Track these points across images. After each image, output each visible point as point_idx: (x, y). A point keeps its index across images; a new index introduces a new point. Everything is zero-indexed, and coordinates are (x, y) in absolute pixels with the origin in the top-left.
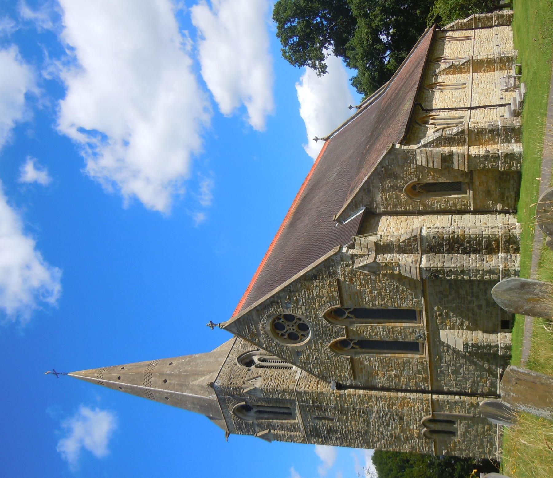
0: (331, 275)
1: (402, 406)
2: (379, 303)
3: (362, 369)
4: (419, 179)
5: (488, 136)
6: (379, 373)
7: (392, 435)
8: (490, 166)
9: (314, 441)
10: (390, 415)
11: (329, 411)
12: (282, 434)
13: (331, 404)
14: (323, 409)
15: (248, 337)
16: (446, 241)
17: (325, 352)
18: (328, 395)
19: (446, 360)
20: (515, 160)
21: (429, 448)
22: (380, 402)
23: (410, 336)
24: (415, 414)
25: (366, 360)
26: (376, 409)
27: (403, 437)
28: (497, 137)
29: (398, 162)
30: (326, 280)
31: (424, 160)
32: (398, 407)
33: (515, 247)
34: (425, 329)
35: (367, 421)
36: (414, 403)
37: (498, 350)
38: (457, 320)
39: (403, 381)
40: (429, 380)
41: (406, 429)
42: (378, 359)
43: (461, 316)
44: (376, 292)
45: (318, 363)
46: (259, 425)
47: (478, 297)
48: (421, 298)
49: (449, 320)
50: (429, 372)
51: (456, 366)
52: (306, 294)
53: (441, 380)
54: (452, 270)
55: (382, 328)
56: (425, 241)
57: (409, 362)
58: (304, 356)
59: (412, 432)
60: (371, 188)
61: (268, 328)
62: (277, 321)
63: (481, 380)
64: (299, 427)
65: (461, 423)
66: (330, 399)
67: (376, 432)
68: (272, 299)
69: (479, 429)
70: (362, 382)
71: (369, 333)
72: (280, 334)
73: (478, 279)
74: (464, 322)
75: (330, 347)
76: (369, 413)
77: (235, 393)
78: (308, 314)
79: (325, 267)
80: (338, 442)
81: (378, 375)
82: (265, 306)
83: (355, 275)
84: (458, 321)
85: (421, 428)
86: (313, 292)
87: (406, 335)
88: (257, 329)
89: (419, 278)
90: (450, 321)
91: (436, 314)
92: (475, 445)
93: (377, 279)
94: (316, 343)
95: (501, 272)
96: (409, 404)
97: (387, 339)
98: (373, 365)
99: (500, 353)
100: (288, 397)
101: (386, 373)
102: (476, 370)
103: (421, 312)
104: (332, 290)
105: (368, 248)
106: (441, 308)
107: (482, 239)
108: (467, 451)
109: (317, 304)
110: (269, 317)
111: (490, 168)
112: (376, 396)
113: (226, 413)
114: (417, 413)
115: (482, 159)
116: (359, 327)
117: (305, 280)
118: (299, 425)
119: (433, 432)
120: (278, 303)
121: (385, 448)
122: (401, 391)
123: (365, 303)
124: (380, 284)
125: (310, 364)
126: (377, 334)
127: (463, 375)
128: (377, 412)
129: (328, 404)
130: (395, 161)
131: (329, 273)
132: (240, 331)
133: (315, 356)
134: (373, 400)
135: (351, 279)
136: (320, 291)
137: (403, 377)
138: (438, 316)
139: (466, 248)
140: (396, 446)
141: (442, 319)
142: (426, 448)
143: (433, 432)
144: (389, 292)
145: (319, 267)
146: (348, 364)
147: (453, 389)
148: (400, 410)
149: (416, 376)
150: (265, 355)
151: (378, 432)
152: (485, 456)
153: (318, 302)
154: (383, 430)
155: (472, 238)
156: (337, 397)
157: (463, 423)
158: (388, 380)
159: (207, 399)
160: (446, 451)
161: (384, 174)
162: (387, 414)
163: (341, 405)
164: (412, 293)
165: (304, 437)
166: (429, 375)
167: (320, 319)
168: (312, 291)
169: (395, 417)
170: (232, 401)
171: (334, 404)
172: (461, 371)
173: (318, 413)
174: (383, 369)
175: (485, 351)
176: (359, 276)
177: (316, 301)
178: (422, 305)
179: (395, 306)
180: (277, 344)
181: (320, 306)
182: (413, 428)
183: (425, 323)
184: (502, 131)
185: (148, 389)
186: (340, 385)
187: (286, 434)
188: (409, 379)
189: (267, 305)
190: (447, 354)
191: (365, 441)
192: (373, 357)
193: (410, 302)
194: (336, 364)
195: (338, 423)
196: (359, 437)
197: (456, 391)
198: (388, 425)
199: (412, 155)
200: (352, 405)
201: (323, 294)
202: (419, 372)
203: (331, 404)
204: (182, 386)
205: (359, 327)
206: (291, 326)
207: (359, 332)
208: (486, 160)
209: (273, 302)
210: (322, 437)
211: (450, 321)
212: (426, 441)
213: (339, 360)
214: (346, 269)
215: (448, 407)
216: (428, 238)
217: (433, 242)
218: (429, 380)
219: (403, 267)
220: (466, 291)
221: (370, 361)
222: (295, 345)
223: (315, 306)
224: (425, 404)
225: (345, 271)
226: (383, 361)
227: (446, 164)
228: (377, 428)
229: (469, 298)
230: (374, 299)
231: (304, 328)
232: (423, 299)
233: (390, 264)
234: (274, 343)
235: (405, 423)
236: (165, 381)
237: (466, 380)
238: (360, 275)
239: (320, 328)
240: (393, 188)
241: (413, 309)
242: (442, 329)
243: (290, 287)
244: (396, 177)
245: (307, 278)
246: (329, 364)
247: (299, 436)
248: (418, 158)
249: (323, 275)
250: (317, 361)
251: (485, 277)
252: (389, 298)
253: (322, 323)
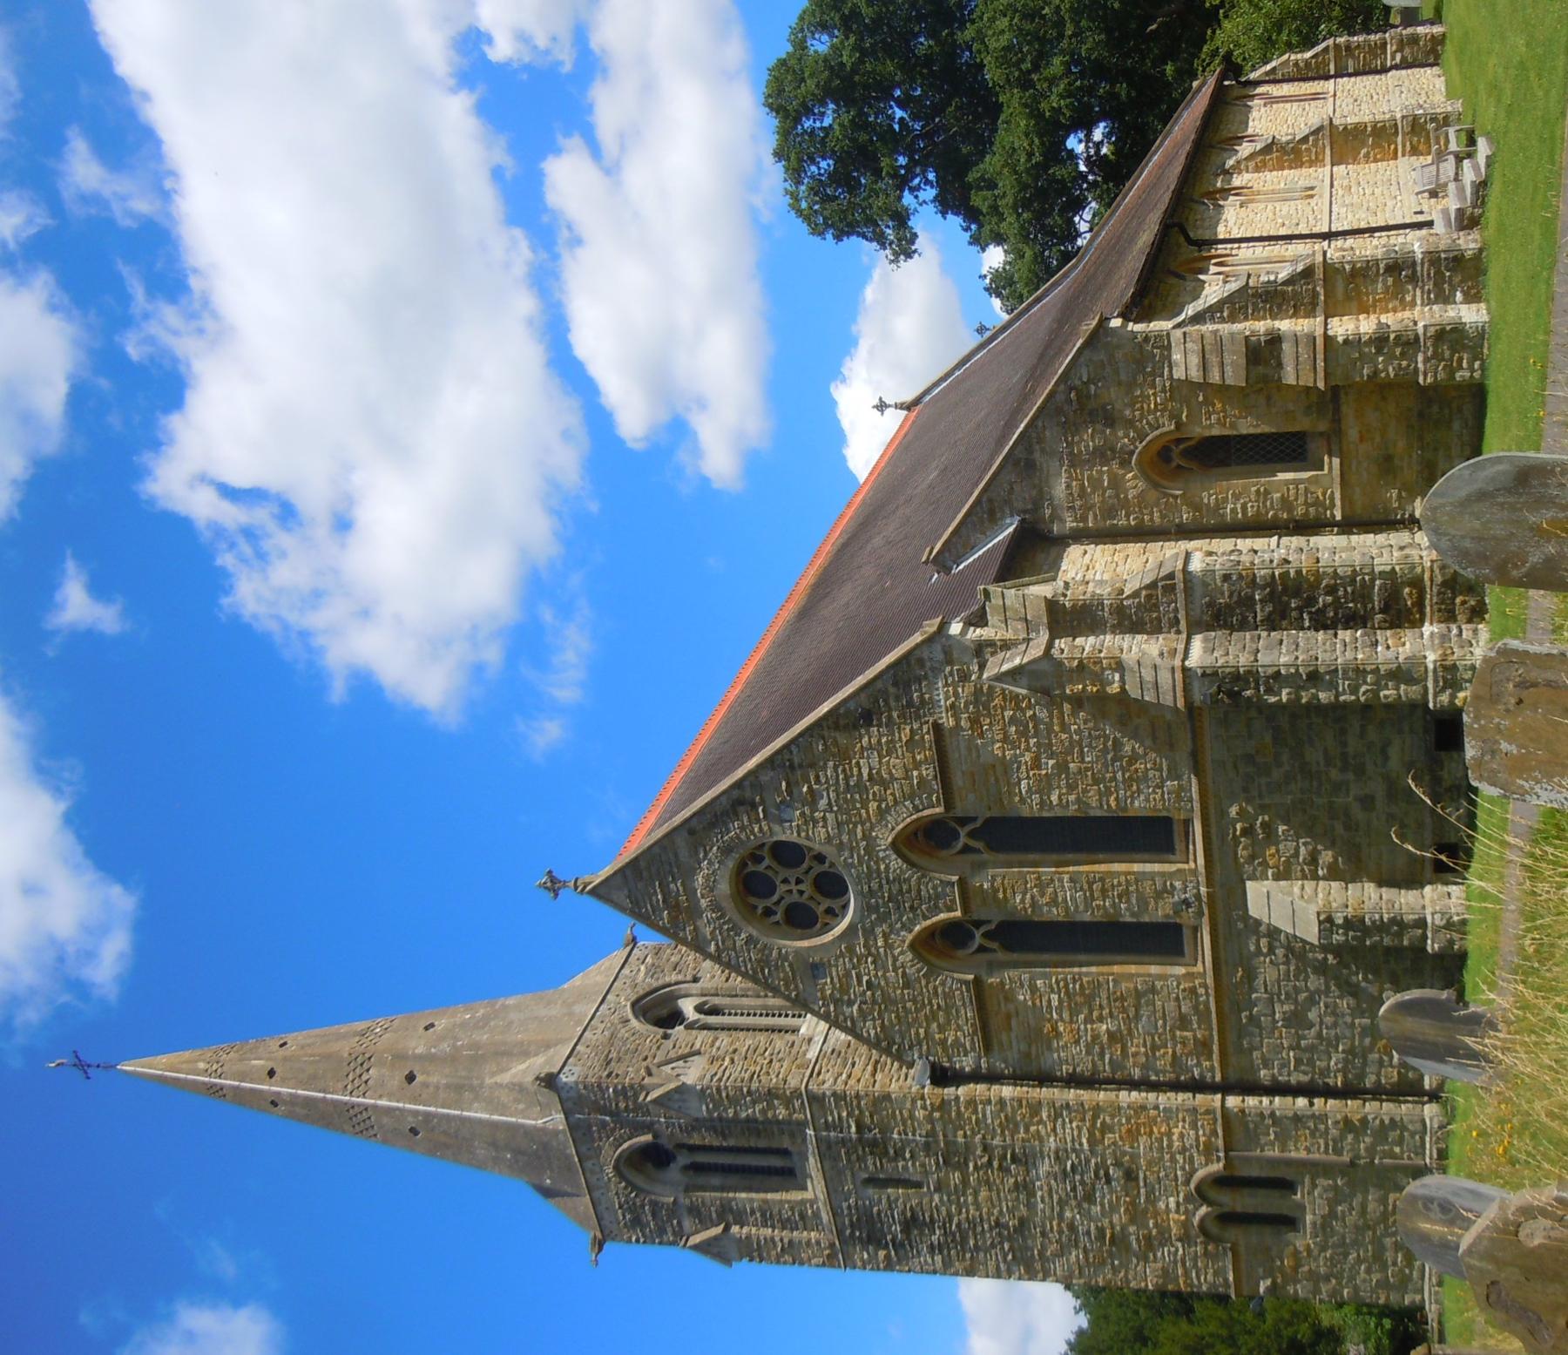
0: (915, 711)
1: (1133, 1135)
2: (1060, 797)
3: (1008, 1017)
4: (1179, 426)
5: (1385, 282)
6: (1061, 1029)
8: (1391, 369)
9: (862, 1259)
10: (1096, 1164)
11: (908, 1155)
12: (765, 1239)
13: (914, 1135)
14: (892, 1152)
15: (662, 919)
16: (1263, 588)
17: (898, 964)
18: (904, 1102)
19: (1265, 981)
20: (1464, 348)
21: (1216, 1274)
23: (1156, 903)
24: (1173, 1160)
25: (1022, 986)
26: (1053, 1145)
27: (1138, 1239)
28: (1410, 287)
29: (1117, 372)
30: (899, 728)
31: (1194, 360)
32: (1121, 1138)
33: (1473, 603)
34: (1202, 879)
35: (1025, 1187)
36: (1168, 1125)
37: (1425, 937)
38: (1297, 849)
39: (1135, 1055)
40: (1215, 1048)
41: (1145, 1211)
42: (1057, 982)
43: (1310, 833)
44: (1051, 762)
45: (874, 1002)
46: (694, 1211)
47: (1360, 771)
48: (1189, 778)
49: (1273, 850)
50: (1214, 1021)
51: (1296, 1000)
52: (838, 776)
53: (1252, 1049)
54: (1283, 672)
55: (1071, 880)
56: (1198, 591)
57: (1153, 990)
58: (832, 979)
59: (1163, 1221)
60: (1037, 455)
61: (724, 887)
62: (751, 868)
63: (1373, 1044)
64: (817, 1215)
65: (1314, 1186)
66: (912, 1117)
67: (1055, 1223)
68: (736, 793)
69: (1371, 1207)
70: (1011, 1062)
71: (1033, 897)
72: (760, 911)
73: (1362, 699)
74: (1319, 852)
75: (912, 946)
76: (1031, 1161)
77: (622, 1105)
78: (845, 838)
79: (895, 684)
80: (938, 1258)
81: (1058, 1035)
82: (716, 815)
83: (986, 707)
84: (1303, 850)
85: (1191, 1207)
86: (860, 769)
87: (1143, 902)
88: (690, 892)
89: (1180, 704)
90: (1278, 851)
91: (1235, 830)
92: (1359, 1261)
93: (1055, 721)
94: (869, 933)
95: (1430, 674)
96: (1155, 1130)
97: (1087, 917)
98: (1044, 1004)
99: (1432, 946)
100: (782, 1113)
101: (1082, 1027)
102: (1357, 1011)
103: (1187, 823)
104: (918, 757)
105: (1026, 620)
106: (1250, 809)
107: (1373, 580)
108: (1334, 1281)
109: (873, 806)
110: (726, 851)
111: (1392, 375)
112: (1052, 1104)
113: (592, 1172)
114: (1178, 1156)
115: (1367, 350)
116: (999, 880)
117: (837, 727)
118: (818, 1208)
119: (1228, 1219)
120: (754, 806)
121: (1080, 1278)
122: (1133, 1085)
123: (1017, 799)
124: (1064, 736)
125: (850, 1003)
126: (1054, 902)
127: (1317, 1027)
128: (1057, 1158)
129: (906, 1134)
130: (1108, 369)
131: (910, 704)
132: (637, 903)
133: (865, 978)
134: (1044, 1115)
135: (975, 722)
136: (880, 762)
137: (1135, 1041)
138: (1242, 835)
139: (1321, 611)
140: (1115, 1270)
141: (1253, 844)
142: (1206, 1274)
143: (1228, 1219)
144: (1092, 762)
145: (879, 684)
146: (967, 1000)
147: (1289, 1075)
148: (1127, 1148)
149: (1173, 1037)
150: (717, 995)
151: (1059, 1225)
152: (1388, 1298)
153: (874, 800)
154: (1074, 1217)
155: (1341, 578)
156: (933, 1110)
157: (1319, 1188)
158: (1088, 1053)
159: (535, 1127)
160: (1269, 1282)
161: (1075, 412)
162: (1088, 1161)
163: (945, 1136)
164: (1161, 764)
165: (832, 1245)
166: (1215, 1033)
167: (881, 854)
168: (858, 763)
169: (1111, 1172)
170: (613, 1130)
171: (924, 1133)
172: (1312, 1015)
173: (875, 1164)
174: (1074, 1013)
175: (1387, 941)
176: (999, 711)
177: (871, 797)
178: (1191, 801)
179: (1109, 805)
180: (750, 940)
181: (882, 813)
182: (1167, 1206)
183: (1201, 860)
184: (1426, 265)
185: (359, 1105)
186: (944, 1070)
187: (777, 1239)
188: (1154, 1048)
189: (722, 814)
190: (1268, 960)
191: (1018, 1254)
192: (1046, 976)
193: (1154, 792)
194: (930, 1003)
195: (936, 1197)
196: (1001, 1243)
197: (1299, 1083)
198: (1089, 1197)
199: (1157, 348)
200: (979, 1136)
201: (890, 773)
202: (1183, 1022)
203: (914, 1135)
204: (460, 1090)
205: (999, 880)
206: (793, 881)
207: (1001, 895)
208: (1379, 351)
209: (740, 802)
210: (886, 1247)
211: (1278, 851)
212: (1206, 1249)
213: (940, 990)
214: (960, 690)
215: (1275, 1133)
216: (1208, 580)
217: (1223, 594)
218: (1215, 1048)
219: (1132, 670)
220: (1326, 751)
221: (1034, 989)
222: (805, 944)
223: (868, 812)
224: (1203, 1126)
225: (956, 694)
226: (1074, 988)
227: (1261, 369)
228: (1057, 1209)
229: (1334, 774)
230: (1044, 785)
231: (831, 886)
233: (1095, 663)
234: (743, 936)
235: (1143, 1191)
236: (411, 1078)
237: (1329, 1044)
238: (1003, 709)
239: (881, 886)
240: (1102, 454)
241: (1164, 814)
242: (1253, 878)
243: (791, 752)
244: (1110, 419)
245: (842, 722)
246: (909, 1005)
247: (818, 1243)
248: (1177, 356)
249: (890, 710)
250: (873, 995)
251: (1382, 694)
252: (1090, 782)
253: (887, 867)
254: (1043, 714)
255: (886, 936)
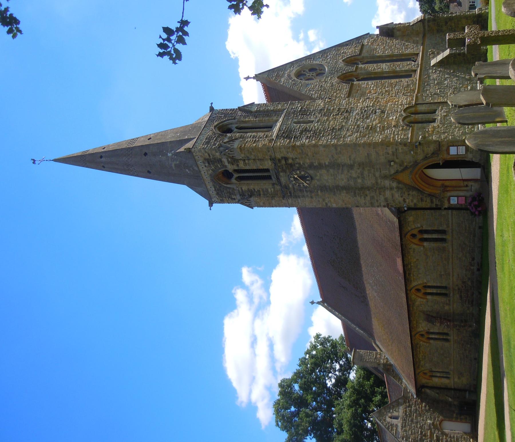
1: (387, 102)
3: (358, 90)
7: (368, 126)
10: (373, 109)
14: (308, 114)
18: (319, 102)
21: (405, 135)
22: (366, 102)
24: (398, 107)
35: (347, 118)
45: (321, 90)
61: (294, 71)
65: (442, 110)
76: (352, 111)
78: (331, 62)
80: (308, 140)
87: (403, 67)
88: (284, 74)
96: (394, 101)
117: (339, 47)
125: (313, 91)
128: (361, 110)
142: (401, 136)
162: (370, 109)
172: (446, 82)
194: (337, 89)
195: (316, 124)
221: (367, 84)
225: (369, 41)
232: (422, 47)
253: (339, 66)
254: (389, 41)
255: (331, 78)
